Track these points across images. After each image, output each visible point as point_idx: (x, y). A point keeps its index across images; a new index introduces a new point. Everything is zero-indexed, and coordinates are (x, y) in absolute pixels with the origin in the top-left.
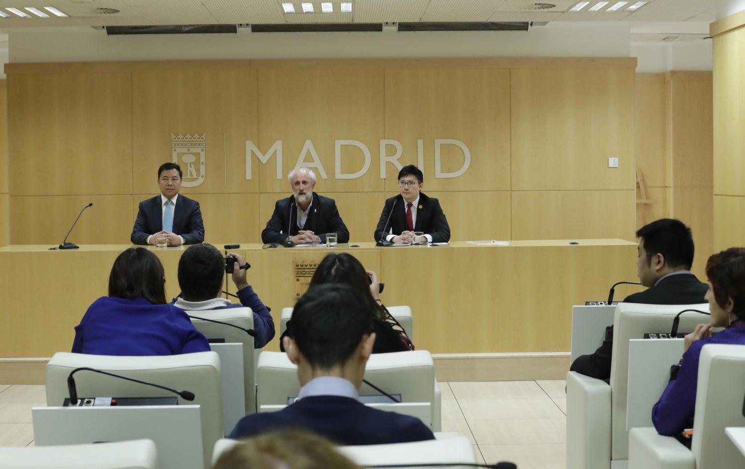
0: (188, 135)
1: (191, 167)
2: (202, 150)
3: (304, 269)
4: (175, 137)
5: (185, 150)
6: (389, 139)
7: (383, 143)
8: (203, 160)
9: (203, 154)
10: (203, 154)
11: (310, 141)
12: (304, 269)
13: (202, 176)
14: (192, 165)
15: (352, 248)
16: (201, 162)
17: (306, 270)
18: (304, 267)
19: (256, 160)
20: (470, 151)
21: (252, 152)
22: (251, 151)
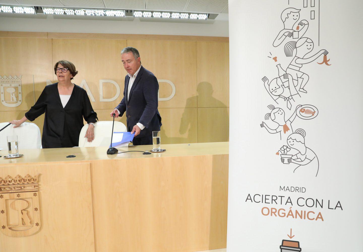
1: (13, 95)
3: (9, 185)
8: (20, 91)
12: (9, 185)
13: (20, 101)
14: (13, 94)
16: (19, 92)
17: (10, 186)
20: (175, 86)
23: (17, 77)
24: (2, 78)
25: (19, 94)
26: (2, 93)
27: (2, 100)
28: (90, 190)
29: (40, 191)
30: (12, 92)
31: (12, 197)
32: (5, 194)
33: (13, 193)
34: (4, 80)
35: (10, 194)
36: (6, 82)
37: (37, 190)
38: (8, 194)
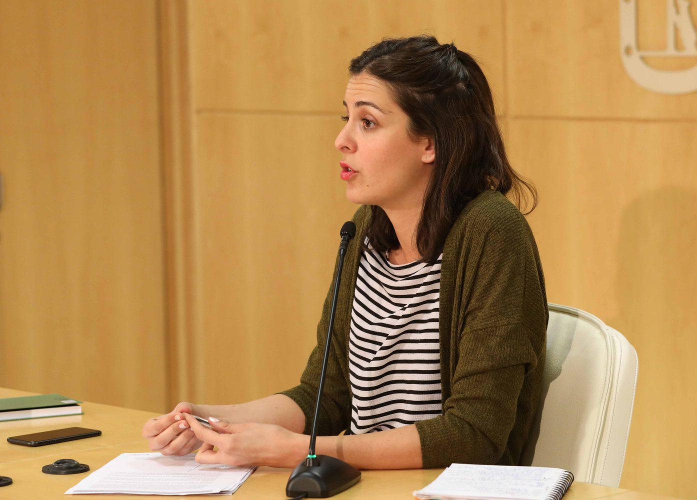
1: (678, 11)
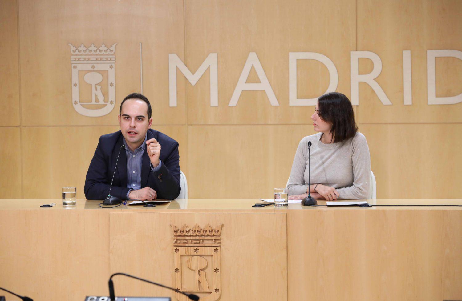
0: (93, 46)
1: (96, 90)
2: (111, 67)
3: (185, 235)
4: (74, 49)
5: (89, 67)
6: (363, 50)
7: (355, 56)
8: (112, 79)
9: (111, 73)
10: (111, 73)
11: (255, 53)
12: (185, 235)
14: (97, 86)
15: (254, 208)
16: (110, 82)
17: (187, 238)
18: (185, 233)
19: (182, 80)
21: (178, 72)
22: (176, 67)
23: (106, 49)
24: (77, 51)
25: (110, 87)
26: (75, 85)
27: (73, 101)
28: (286, 250)
29: (222, 247)
30: (96, 83)
31: (189, 253)
32: (181, 247)
33: (190, 247)
34: (80, 55)
35: (187, 247)
36: (85, 59)
37: (219, 245)
38: (185, 247)
